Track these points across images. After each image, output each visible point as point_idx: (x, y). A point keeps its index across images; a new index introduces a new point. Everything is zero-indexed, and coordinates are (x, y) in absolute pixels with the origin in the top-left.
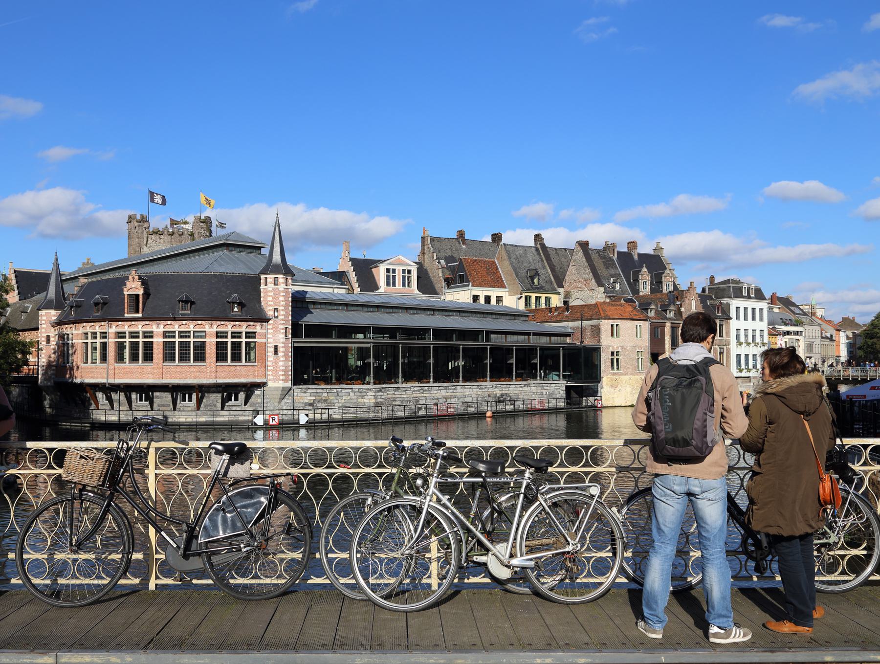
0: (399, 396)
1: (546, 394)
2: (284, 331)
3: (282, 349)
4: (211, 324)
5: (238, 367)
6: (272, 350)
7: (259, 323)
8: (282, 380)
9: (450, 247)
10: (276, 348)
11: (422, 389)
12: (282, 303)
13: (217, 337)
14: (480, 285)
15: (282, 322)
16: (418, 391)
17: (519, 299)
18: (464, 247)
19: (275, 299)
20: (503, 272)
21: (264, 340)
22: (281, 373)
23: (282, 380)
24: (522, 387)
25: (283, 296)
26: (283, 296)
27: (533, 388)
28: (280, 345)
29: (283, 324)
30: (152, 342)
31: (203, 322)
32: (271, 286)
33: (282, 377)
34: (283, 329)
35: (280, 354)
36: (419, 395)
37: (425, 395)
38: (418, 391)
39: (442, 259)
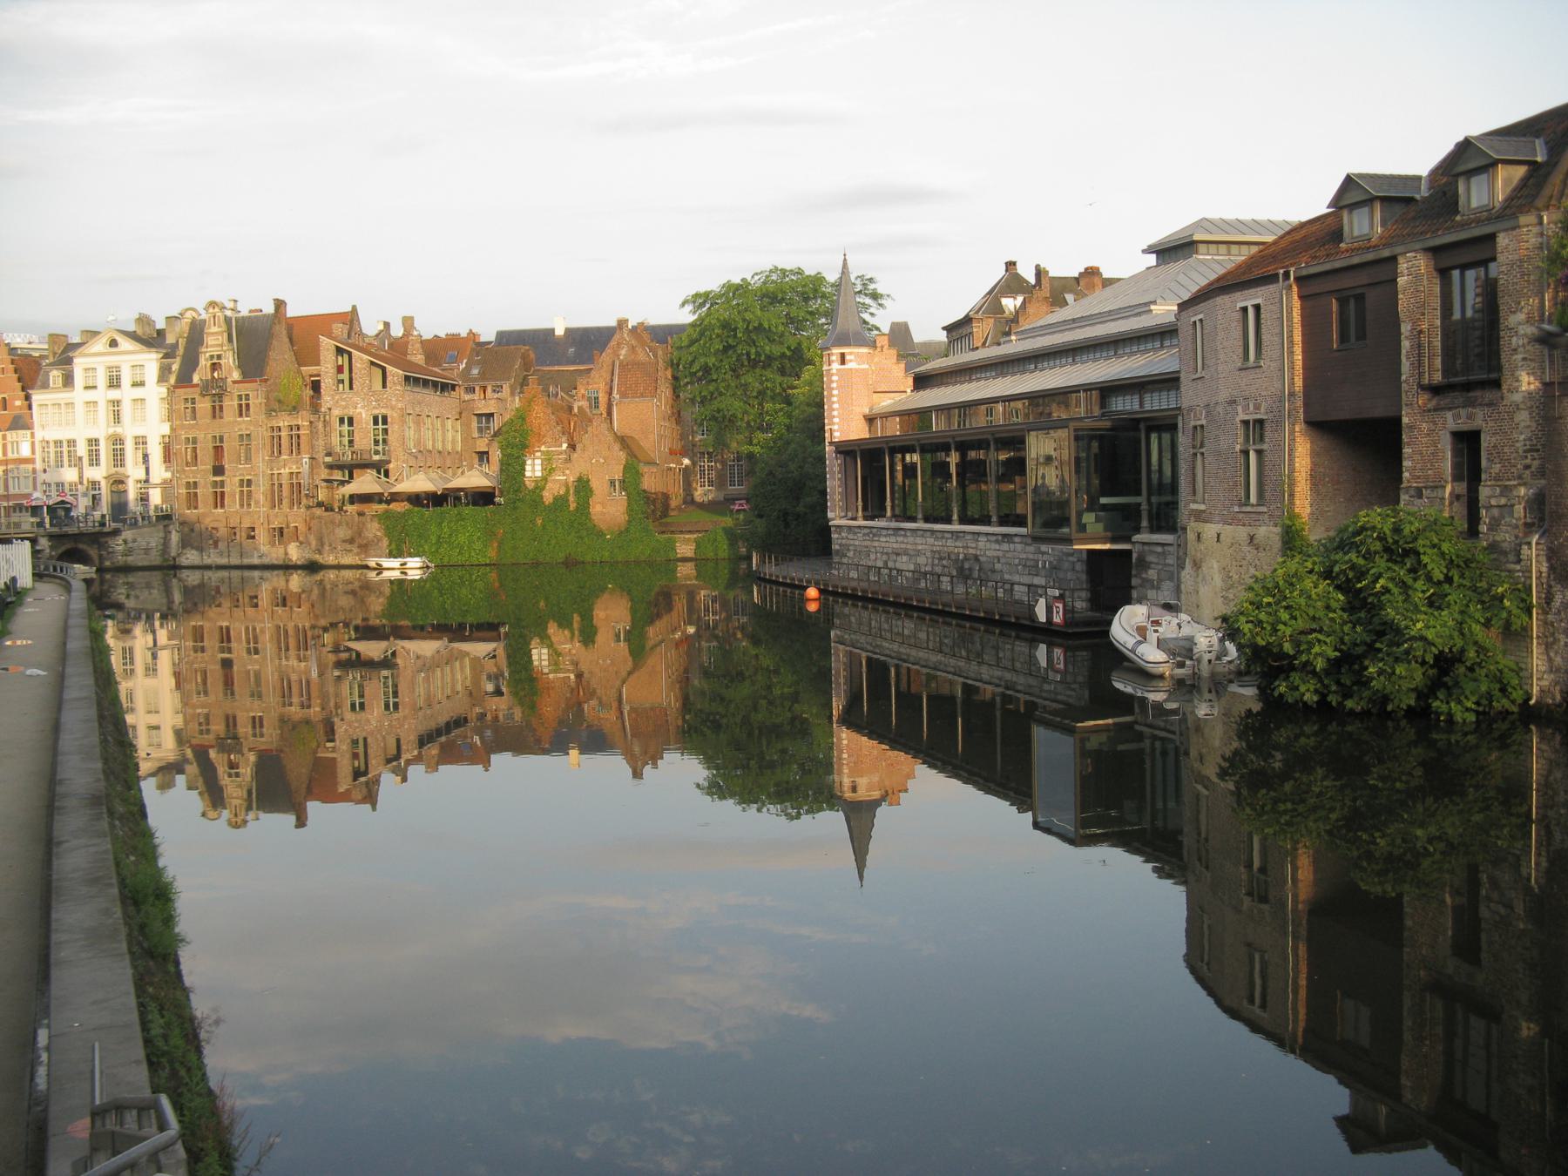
0: (852, 542)
1: (1044, 567)
11: (871, 532)
16: (868, 534)
24: (997, 542)
27: (1019, 547)
32: (836, 366)
36: (868, 543)
37: (876, 544)
38: (868, 534)
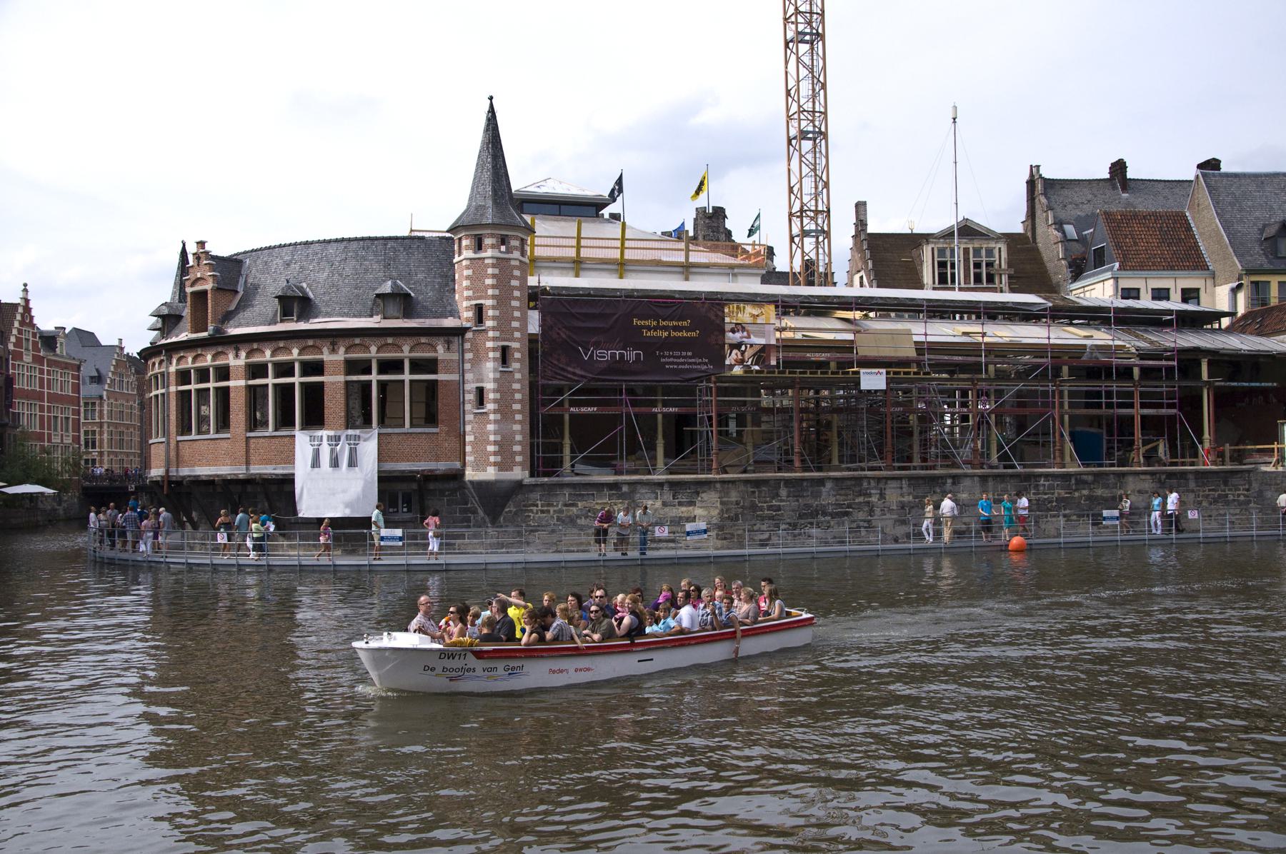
2: (498, 355)
3: (491, 396)
4: (333, 344)
5: (395, 438)
6: (470, 397)
7: (442, 339)
8: (495, 464)
9: (1090, 197)
10: (480, 392)
12: (490, 292)
13: (348, 373)
14: (1142, 267)
15: (491, 334)
17: (1239, 287)
18: (1125, 195)
19: (476, 279)
20: (1201, 234)
21: (455, 377)
22: (517, 448)
23: (495, 464)
25: (494, 276)
26: (494, 276)
28: (489, 386)
29: (494, 339)
30: (228, 388)
31: (319, 342)
33: (492, 459)
34: (494, 349)
35: (490, 406)
39: (1069, 223)
